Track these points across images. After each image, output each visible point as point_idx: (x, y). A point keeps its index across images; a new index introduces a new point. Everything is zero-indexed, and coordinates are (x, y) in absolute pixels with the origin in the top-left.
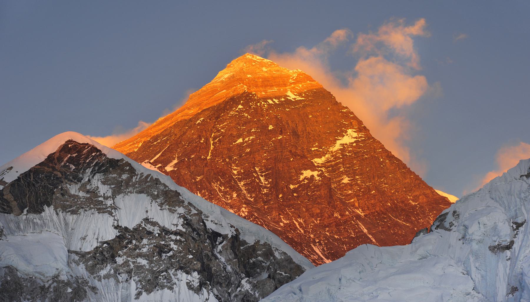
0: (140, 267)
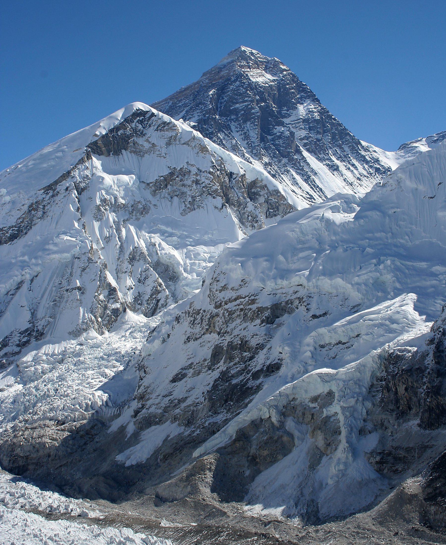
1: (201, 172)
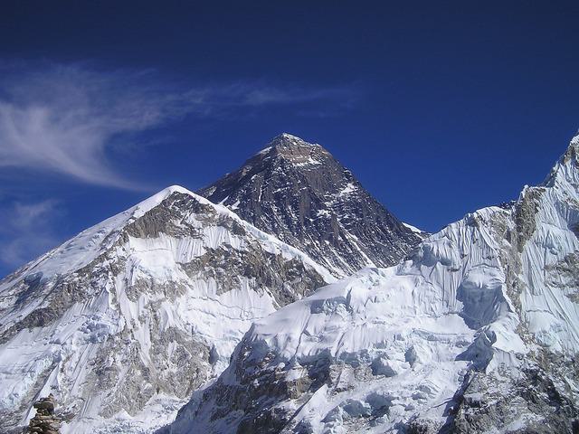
0: (219, 274)
1: (237, 251)
